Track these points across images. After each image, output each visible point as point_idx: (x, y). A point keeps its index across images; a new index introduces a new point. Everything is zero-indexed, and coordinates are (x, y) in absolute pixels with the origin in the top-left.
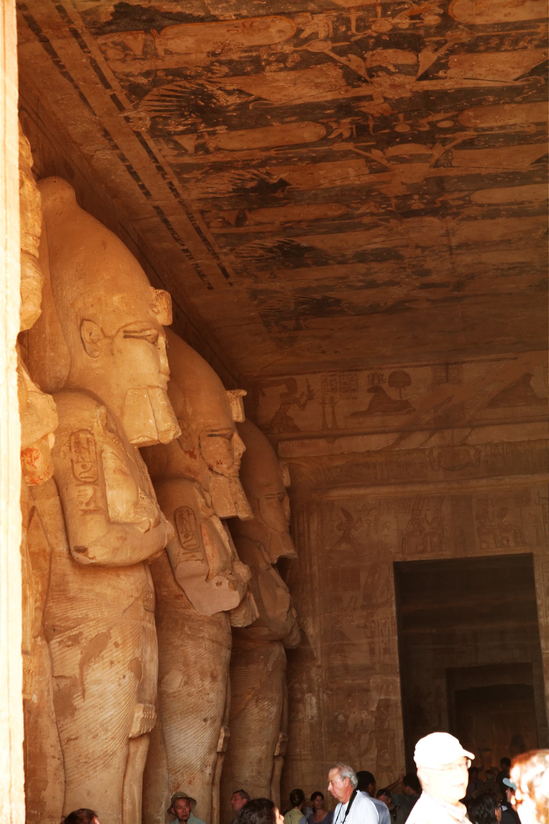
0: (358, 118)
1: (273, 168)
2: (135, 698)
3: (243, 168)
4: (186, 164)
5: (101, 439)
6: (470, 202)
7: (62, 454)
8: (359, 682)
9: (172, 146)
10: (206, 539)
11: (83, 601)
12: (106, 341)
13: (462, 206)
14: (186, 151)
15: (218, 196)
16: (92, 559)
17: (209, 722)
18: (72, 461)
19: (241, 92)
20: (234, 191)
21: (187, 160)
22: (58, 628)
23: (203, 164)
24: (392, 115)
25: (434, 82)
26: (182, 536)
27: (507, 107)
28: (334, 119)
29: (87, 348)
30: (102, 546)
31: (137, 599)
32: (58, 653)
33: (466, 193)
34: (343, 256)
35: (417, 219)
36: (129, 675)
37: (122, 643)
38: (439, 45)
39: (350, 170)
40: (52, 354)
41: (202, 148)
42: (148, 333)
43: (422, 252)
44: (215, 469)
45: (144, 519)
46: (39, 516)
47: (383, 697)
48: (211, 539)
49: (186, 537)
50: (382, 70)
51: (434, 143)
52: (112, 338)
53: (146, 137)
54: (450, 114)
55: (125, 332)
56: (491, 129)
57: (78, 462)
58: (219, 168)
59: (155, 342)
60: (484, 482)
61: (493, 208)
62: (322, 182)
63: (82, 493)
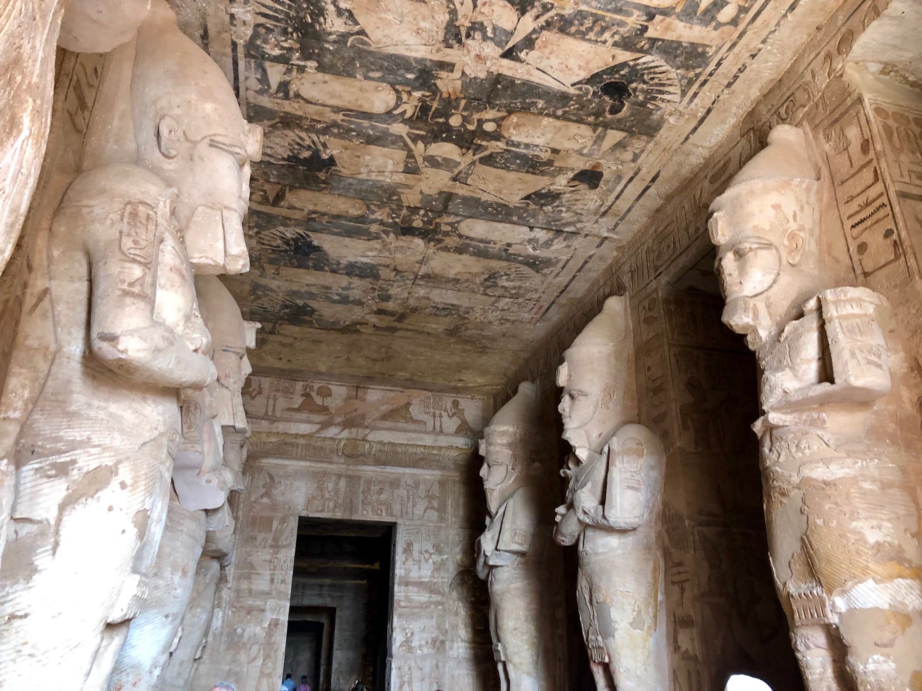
0: (428, 94)
1: (332, 138)
2: (131, 565)
3: (307, 131)
4: (262, 107)
5: (165, 224)
6: (456, 229)
7: (108, 222)
8: (258, 603)
9: (259, 76)
10: (206, 436)
11: (88, 420)
12: (186, 145)
13: (446, 234)
14: (269, 87)
15: (272, 161)
16: (122, 352)
17: (170, 619)
18: (121, 232)
19: (351, 15)
20: (289, 159)
21: (265, 101)
22: (40, 450)
23: (276, 112)
24: (457, 99)
25: (512, 64)
26: (185, 427)
27: (546, 121)
28: (408, 89)
29: (163, 144)
30: (141, 337)
31: (161, 434)
32: (29, 485)
33: (459, 219)
34: (339, 264)
35: (408, 238)
36: (133, 531)
37: (132, 485)
38: (546, 8)
39: (391, 162)
40: (115, 147)
41: (284, 87)
42: (238, 150)
43: (396, 275)
44: (222, 381)
45: (194, 336)
46: (51, 301)
47: (274, 617)
48: (210, 438)
49: (189, 428)
50: (481, 31)
51: (468, 149)
52: (195, 143)
53: (241, 51)
54: (500, 114)
55: (211, 140)
56: (518, 145)
57: (129, 235)
58: (288, 122)
59: (242, 166)
60: (372, 468)
61: (468, 241)
62: (362, 170)
63: (127, 270)
